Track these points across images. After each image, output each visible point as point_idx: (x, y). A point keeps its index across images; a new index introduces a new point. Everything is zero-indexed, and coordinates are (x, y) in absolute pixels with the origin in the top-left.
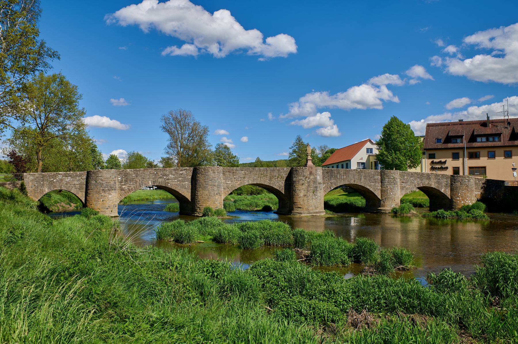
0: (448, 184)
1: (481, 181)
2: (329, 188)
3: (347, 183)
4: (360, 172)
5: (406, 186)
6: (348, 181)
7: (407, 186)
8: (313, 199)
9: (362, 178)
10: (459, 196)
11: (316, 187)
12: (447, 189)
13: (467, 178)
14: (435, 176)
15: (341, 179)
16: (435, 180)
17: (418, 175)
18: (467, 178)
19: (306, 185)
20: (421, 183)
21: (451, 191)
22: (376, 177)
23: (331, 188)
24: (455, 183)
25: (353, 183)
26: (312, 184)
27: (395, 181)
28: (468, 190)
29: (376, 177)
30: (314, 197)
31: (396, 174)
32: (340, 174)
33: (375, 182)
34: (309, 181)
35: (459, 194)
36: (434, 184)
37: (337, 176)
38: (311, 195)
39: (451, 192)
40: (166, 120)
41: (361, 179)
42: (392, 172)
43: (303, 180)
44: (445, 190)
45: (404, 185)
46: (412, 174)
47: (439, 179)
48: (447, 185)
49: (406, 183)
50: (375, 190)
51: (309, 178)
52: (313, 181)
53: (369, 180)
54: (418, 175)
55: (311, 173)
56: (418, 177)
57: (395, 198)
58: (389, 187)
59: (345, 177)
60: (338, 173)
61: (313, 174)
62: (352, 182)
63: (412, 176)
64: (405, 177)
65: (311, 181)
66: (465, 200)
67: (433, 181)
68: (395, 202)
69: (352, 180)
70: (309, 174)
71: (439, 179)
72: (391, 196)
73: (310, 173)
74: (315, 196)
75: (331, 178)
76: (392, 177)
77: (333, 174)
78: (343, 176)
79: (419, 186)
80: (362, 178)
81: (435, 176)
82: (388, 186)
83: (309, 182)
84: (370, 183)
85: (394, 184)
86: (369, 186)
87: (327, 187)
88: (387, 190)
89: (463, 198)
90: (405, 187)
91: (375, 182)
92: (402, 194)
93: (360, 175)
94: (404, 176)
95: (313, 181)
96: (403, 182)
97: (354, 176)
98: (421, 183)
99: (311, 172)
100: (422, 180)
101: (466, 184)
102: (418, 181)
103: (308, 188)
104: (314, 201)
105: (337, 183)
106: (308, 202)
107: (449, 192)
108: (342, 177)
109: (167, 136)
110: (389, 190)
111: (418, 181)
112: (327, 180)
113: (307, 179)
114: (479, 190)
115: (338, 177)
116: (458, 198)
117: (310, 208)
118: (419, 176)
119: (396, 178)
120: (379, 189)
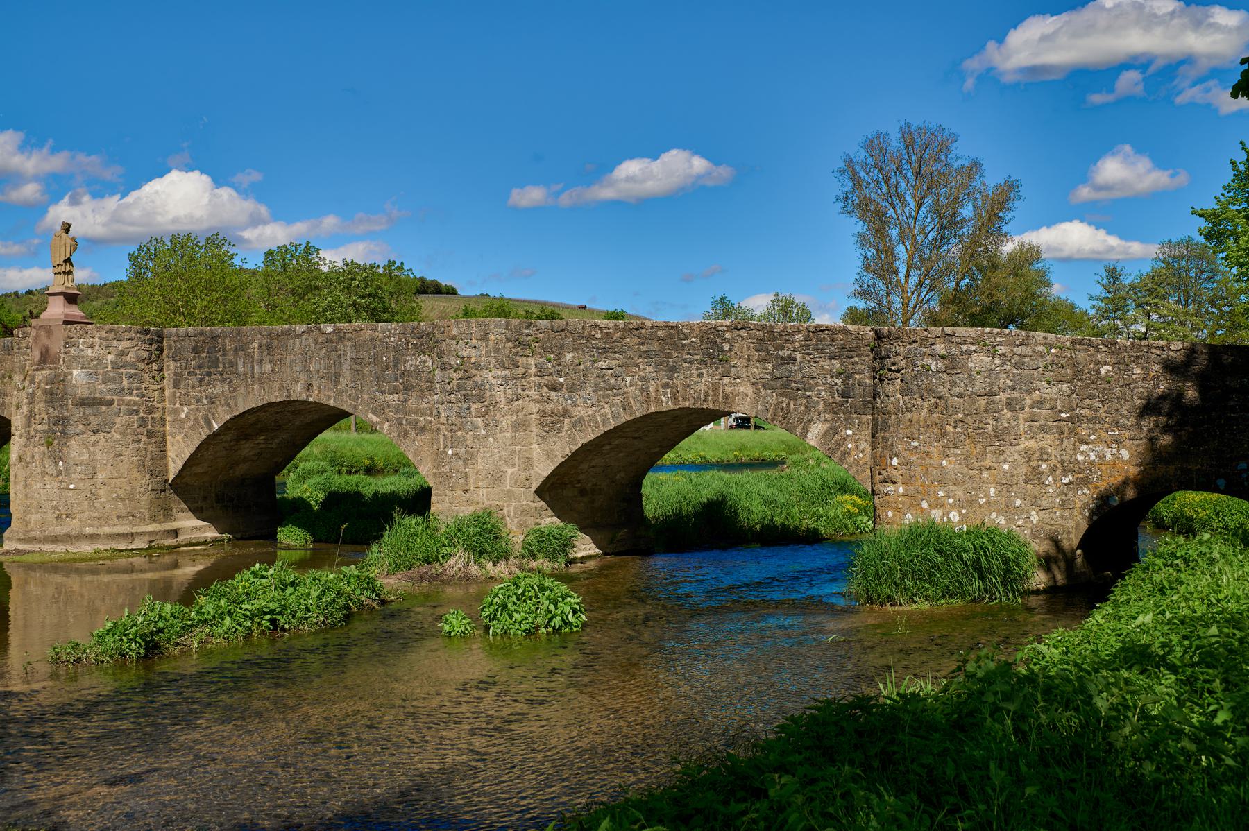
0: (858, 390)
1: (1136, 361)
2: (202, 423)
3: (277, 397)
4: (335, 338)
5: (574, 411)
6: (281, 388)
7: (581, 411)
8: (44, 473)
9: (346, 370)
10: (895, 474)
11: (63, 421)
12: (848, 423)
13: (940, 349)
14: (761, 340)
15: (253, 377)
16: (757, 370)
17: (644, 340)
18: (940, 349)
19: (25, 409)
20: (666, 386)
21: (873, 437)
22: (412, 362)
23: (209, 425)
24: (881, 380)
25: (303, 397)
26: (41, 405)
27: (469, 383)
28: (944, 434)
29: (412, 362)
30: (50, 469)
31: (474, 342)
32: (247, 355)
33: (406, 389)
34: (30, 391)
35: (895, 462)
36: (749, 390)
37: (233, 364)
38: (37, 457)
39: (873, 447)
40: (849, 169)
41: (338, 376)
42: (455, 332)
43: (18, 389)
44: (834, 431)
45: (558, 401)
46: (607, 337)
47: (790, 360)
48: (845, 395)
49: (571, 389)
50: (406, 434)
51: (33, 381)
52: (45, 392)
53: (379, 379)
54: (644, 340)
55: (46, 357)
56: (647, 355)
57: (466, 476)
58: (443, 419)
59: (267, 367)
60: (241, 348)
61: (55, 360)
62: (298, 393)
63: (606, 351)
64: (569, 357)
65: (39, 393)
66: (925, 505)
67: (743, 372)
68: (469, 503)
69: (296, 381)
70: (37, 359)
71: (790, 360)
72: (447, 468)
73: (41, 353)
74: (56, 464)
75: (209, 374)
76: (455, 361)
77: (219, 355)
78: (261, 361)
79: (653, 409)
80: (346, 370)
81: (761, 340)
82: (442, 408)
83: (32, 397)
84: (383, 393)
85: (467, 398)
86: (374, 412)
87: (196, 419)
88: (438, 430)
89: (911, 491)
90: (566, 413)
91: (406, 389)
92: (549, 455)
93: (333, 356)
94: (562, 347)
95: (45, 392)
96: (554, 388)
97: (306, 359)
98: (666, 386)
99: (47, 350)
100: (673, 369)
101: (929, 391)
102: (643, 379)
103: (29, 426)
104: (50, 483)
105: (235, 397)
106: (26, 486)
107: (865, 446)
108: (256, 368)
109: (856, 226)
110: (443, 431)
111: (643, 379)
112: (197, 384)
113: (27, 383)
114: (1124, 428)
115: (241, 369)
116: (890, 488)
117: (34, 518)
118: (655, 345)
119: (477, 366)
120: (423, 430)
